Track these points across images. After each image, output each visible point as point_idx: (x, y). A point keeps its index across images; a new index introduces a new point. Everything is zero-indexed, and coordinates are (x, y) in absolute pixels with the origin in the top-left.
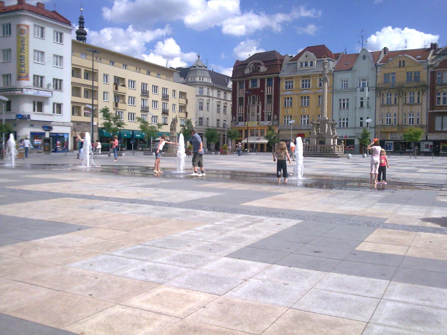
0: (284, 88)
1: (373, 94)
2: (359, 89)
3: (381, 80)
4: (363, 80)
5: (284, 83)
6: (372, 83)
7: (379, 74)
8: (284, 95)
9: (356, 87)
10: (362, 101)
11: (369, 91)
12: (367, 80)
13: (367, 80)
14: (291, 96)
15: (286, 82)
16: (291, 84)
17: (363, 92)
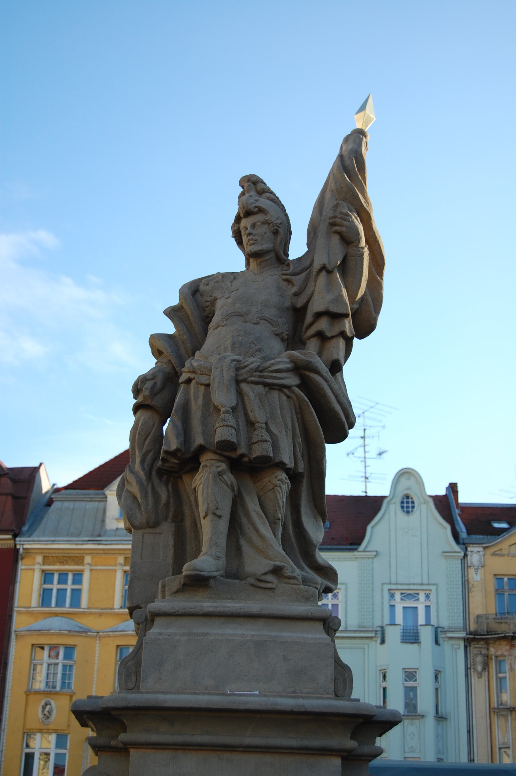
0: (35, 600)
1: (455, 656)
2: (393, 635)
3: (483, 604)
4: (406, 596)
5: (37, 576)
6: (448, 615)
7: (475, 577)
8: (39, 632)
9: (378, 623)
10: (411, 684)
11: (437, 642)
12: (422, 596)
13: (422, 596)
14: (70, 641)
15: (47, 576)
16: (69, 587)
17: (416, 645)
